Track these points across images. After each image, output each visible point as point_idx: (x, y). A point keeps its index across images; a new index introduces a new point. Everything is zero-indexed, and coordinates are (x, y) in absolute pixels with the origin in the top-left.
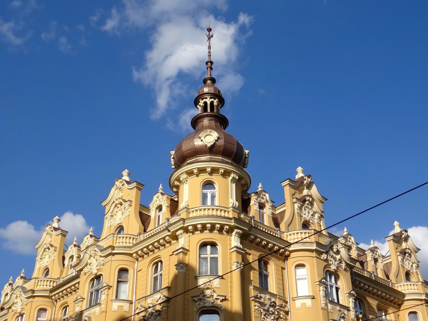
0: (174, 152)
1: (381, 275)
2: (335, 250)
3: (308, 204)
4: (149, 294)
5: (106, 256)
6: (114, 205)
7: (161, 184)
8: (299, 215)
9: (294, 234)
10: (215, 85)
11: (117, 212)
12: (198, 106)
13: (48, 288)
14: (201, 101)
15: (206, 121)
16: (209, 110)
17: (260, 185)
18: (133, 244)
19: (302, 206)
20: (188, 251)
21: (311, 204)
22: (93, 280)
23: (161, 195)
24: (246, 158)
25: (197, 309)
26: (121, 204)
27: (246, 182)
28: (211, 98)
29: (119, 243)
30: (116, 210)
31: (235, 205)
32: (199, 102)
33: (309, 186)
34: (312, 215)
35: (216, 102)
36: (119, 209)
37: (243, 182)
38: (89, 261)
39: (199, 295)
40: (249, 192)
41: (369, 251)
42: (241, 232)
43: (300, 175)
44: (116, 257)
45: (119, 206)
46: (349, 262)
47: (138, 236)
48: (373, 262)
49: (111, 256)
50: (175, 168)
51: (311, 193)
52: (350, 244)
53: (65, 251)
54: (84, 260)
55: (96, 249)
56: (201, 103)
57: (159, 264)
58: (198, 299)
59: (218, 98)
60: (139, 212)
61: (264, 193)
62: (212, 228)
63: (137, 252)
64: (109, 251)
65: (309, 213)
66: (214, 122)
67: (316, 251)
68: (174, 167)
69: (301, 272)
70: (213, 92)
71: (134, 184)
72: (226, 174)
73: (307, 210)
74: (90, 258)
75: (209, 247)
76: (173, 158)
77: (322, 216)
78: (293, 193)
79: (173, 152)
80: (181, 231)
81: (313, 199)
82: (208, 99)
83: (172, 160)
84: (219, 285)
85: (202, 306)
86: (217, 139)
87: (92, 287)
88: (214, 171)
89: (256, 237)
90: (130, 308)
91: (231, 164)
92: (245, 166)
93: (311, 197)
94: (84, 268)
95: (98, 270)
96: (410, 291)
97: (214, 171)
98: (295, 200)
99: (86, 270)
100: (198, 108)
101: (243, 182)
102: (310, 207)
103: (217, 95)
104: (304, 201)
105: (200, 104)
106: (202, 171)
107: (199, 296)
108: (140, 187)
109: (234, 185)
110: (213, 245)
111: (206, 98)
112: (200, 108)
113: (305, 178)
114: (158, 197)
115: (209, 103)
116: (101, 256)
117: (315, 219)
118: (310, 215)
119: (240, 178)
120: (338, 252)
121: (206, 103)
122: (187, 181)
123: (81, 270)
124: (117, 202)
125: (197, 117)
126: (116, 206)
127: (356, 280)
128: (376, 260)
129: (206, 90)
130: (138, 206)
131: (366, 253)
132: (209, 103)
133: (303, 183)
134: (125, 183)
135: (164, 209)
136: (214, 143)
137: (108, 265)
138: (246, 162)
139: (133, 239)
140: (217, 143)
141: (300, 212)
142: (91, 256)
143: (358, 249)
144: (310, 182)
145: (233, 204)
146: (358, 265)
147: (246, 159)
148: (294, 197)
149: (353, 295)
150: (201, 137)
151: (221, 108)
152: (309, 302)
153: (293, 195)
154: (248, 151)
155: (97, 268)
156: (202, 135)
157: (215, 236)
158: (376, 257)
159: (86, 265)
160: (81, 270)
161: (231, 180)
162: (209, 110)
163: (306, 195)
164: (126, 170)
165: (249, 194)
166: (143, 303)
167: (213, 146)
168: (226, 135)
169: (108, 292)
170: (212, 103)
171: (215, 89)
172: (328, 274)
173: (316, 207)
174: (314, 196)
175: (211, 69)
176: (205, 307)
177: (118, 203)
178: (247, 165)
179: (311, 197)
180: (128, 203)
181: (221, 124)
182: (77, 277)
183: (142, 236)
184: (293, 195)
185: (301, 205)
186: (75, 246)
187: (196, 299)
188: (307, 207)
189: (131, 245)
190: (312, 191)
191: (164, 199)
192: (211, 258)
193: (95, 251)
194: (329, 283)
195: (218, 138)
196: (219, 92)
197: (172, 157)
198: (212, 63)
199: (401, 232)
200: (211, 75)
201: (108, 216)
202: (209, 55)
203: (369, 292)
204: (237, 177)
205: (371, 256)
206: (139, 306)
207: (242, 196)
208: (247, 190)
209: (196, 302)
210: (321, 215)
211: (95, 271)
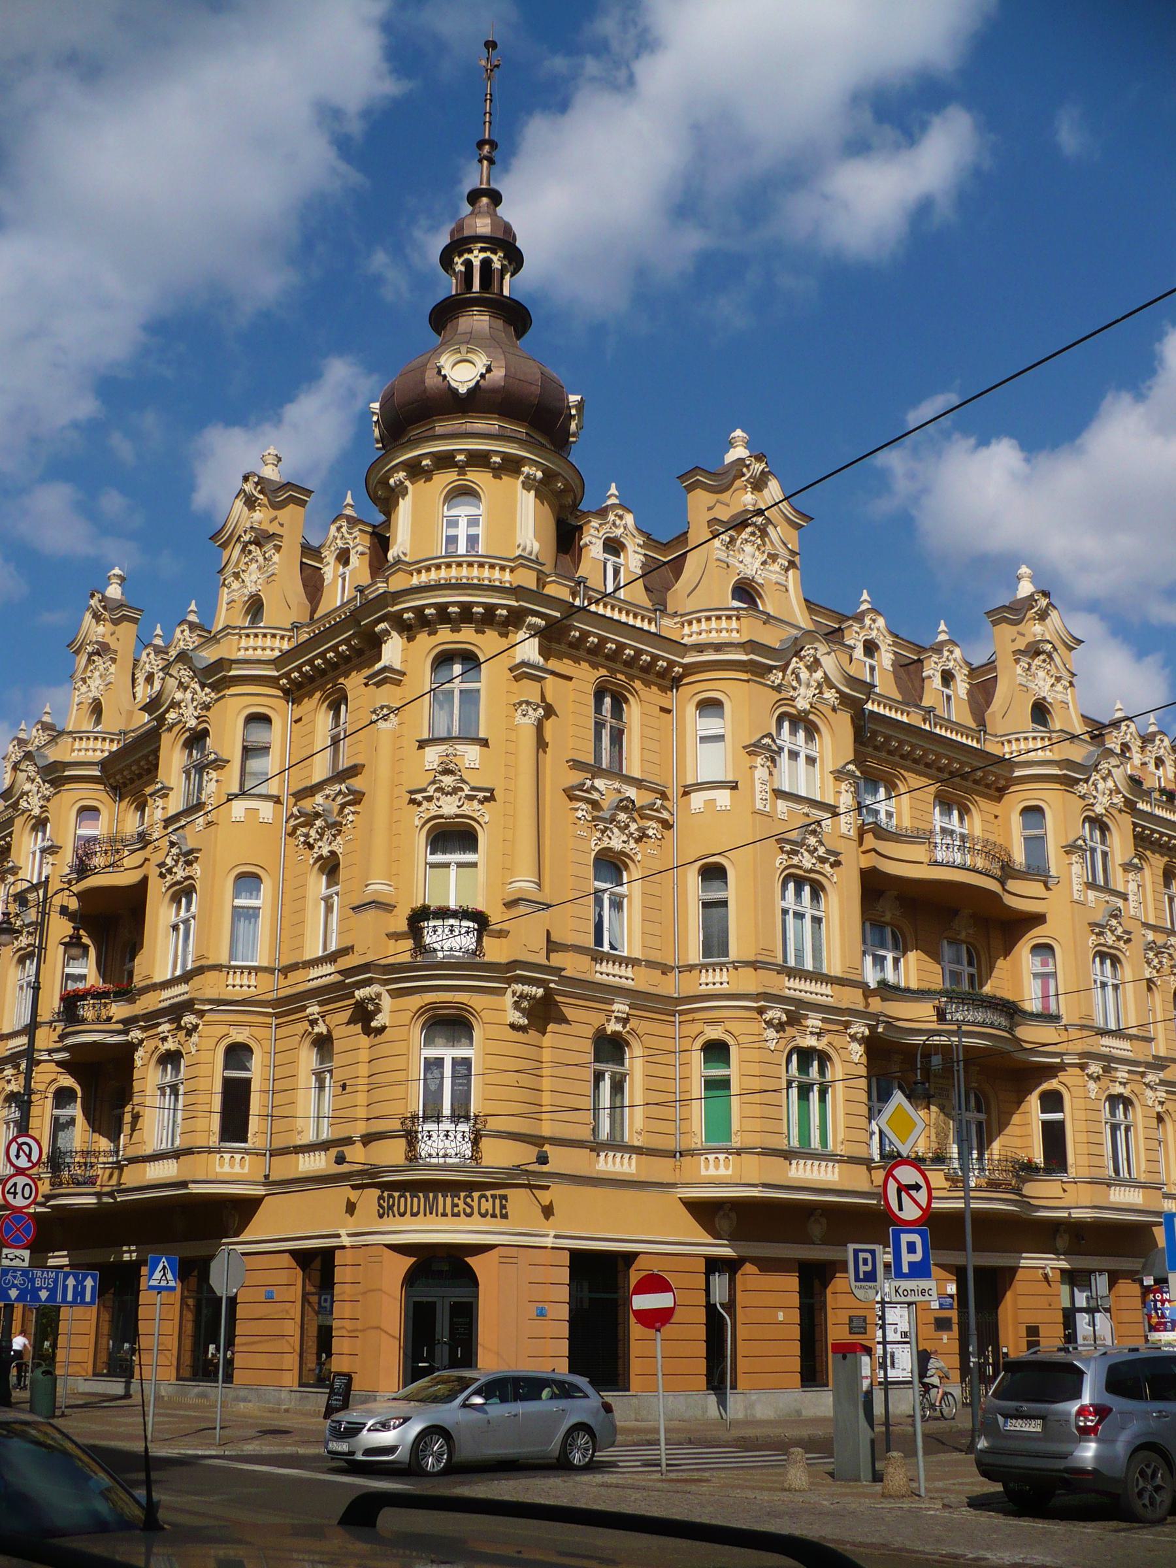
3: (753, 534)
6: (239, 547)
7: (349, 493)
10: (500, 210)
13: (99, 756)
16: (476, 286)
17: (613, 490)
20: (404, 674)
25: (423, 820)
28: (482, 250)
31: (528, 549)
33: (758, 485)
34: (764, 563)
39: (424, 786)
42: (541, 623)
43: (739, 452)
45: (252, 548)
46: (847, 690)
47: (292, 629)
50: (384, 447)
57: (343, 707)
58: (424, 798)
61: (620, 512)
62: (466, 615)
66: (487, 318)
72: (511, 466)
75: (457, 669)
80: (382, 626)
84: (477, 762)
85: (433, 813)
88: (479, 460)
89: (585, 634)
95: (197, 718)
106: (445, 461)
107: (424, 790)
109: (533, 492)
110: (470, 660)
111: (470, 251)
115: (476, 263)
119: (549, 475)
120: (815, 665)
126: (243, 550)
132: (476, 263)
135: (354, 559)
139: (282, 637)
145: (524, 550)
149: (851, 774)
154: (578, 398)
155: (196, 714)
157: (467, 635)
162: (476, 286)
170: (486, 263)
172: (786, 724)
176: (441, 817)
187: (419, 797)
189: (277, 653)
192: (461, 691)
198: (493, 144)
199: (1032, 595)
200: (488, 182)
204: (539, 474)
209: (420, 804)
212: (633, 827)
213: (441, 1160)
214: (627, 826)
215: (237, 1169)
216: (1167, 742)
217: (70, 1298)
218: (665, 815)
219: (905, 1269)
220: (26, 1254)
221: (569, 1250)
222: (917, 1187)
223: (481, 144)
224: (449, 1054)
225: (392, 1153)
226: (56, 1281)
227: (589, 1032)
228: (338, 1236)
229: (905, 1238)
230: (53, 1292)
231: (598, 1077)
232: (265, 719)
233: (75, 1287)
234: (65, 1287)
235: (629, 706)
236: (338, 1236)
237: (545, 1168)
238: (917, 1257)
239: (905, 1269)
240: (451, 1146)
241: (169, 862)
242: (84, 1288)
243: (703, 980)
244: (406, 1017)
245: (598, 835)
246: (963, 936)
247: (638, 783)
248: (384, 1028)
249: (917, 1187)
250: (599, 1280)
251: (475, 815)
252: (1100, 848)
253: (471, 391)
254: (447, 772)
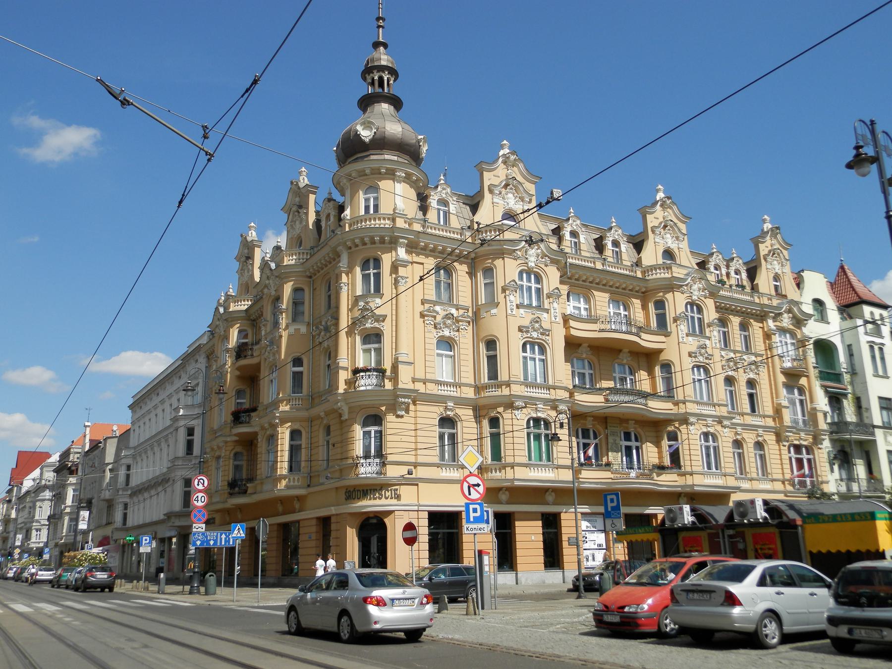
115: (376, 78)
132: (376, 78)
198: (384, 19)
215: (296, 483)
216: (741, 261)
219: (472, 519)
220: (204, 526)
222: (478, 485)
223: (378, 19)
229: (471, 507)
230: (215, 541)
231: (441, 437)
234: (221, 539)
238: (478, 514)
239: (472, 519)
246: (625, 361)
249: (478, 485)
252: (696, 316)
253: (371, 141)
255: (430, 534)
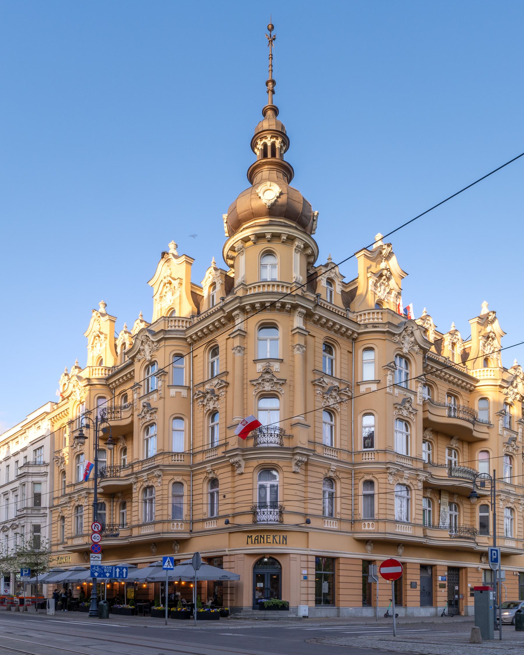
0: (227, 215)
1: (457, 360)
2: (409, 332)
4: (206, 380)
5: (159, 341)
6: (162, 284)
8: (373, 293)
9: (365, 314)
11: (166, 293)
12: (256, 150)
14: (259, 141)
15: (265, 172)
18: (186, 327)
19: (377, 282)
21: (389, 279)
22: (147, 366)
23: (213, 271)
24: (314, 220)
25: (256, 393)
26: (170, 283)
27: (313, 252)
29: (172, 327)
30: (165, 290)
32: (257, 143)
35: (278, 145)
36: (168, 288)
37: (309, 251)
38: (142, 348)
40: (316, 265)
41: (448, 334)
44: (168, 343)
45: (168, 285)
48: (451, 346)
49: (163, 341)
51: (389, 266)
52: (427, 326)
53: (116, 339)
54: (136, 346)
55: (147, 334)
56: (260, 146)
59: (281, 137)
60: (192, 292)
63: (191, 337)
64: (161, 336)
65: (385, 290)
67: (388, 332)
68: (227, 235)
69: (369, 356)
70: (274, 128)
71: (183, 258)
73: (383, 287)
74: (142, 344)
76: (226, 222)
77: (399, 294)
78: (369, 266)
79: (225, 216)
81: (391, 273)
82: (269, 138)
83: (225, 225)
85: (261, 390)
86: (278, 195)
87: (148, 374)
90: (189, 394)
91: (296, 228)
92: (313, 232)
93: (389, 271)
94: (137, 354)
95: (151, 356)
96: (486, 377)
97: (276, 236)
98: (369, 275)
99: (139, 356)
100: (256, 154)
101: (309, 251)
102: (387, 283)
103: (281, 133)
104: (381, 276)
105: (258, 146)
108: (190, 261)
112: (258, 153)
113: (384, 247)
114: (210, 273)
116: (153, 342)
117: (391, 297)
118: (386, 293)
121: (265, 145)
122: (243, 251)
123: (134, 356)
124: (166, 281)
125: (254, 165)
126: (165, 285)
127: (428, 365)
128: (454, 344)
129: (266, 125)
130: (190, 285)
131: (444, 336)
133: (381, 253)
134: (172, 257)
136: (276, 201)
137: (162, 350)
138: (314, 226)
139: (187, 322)
140: (279, 200)
141: (375, 289)
142: (142, 342)
143: (436, 332)
144: (390, 253)
146: (433, 349)
147: (315, 223)
148: (369, 270)
150: (259, 192)
151: (285, 152)
152: (374, 387)
153: (368, 268)
156: (260, 190)
158: (455, 341)
159: (139, 352)
160: (134, 356)
161: (295, 249)
163: (383, 269)
164: (173, 242)
165: (315, 268)
166: (201, 389)
167: (273, 205)
168: (290, 190)
169: (164, 378)
171: (277, 123)
173: (392, 283)
174: (393, 270)
175: (273, 92)
176: (265, 391)
177: (166, 282)
178: (314, 230)
179: (389, 271)
180: (178, 281)
181: (285, 175)
182: (131, 364)
183: (195, 318)
184: (368, 268)
185: (376, 280)
186: (126, 332)
187: (255, 383)
188: (383, 283)
189: (184, 328)
190: (390, 262)
191: (218, 275)
193: (146, 335)
194: (398, 367)
195: (281, 194)
196: (283, 127)
197: (225, 221)
201: (157, 297)
202: (270, 69)
203: (441, 378)
205: (449, 340)
206: (197, 392)
207: (308, 270)
208: (315, 260)
210: (398, 293)
211: (149, 358)
212: (338, 398)
213: (266, 522)
214: (336, 397)
217: (118, 576)
218: (350, 394)
221: (315, 556)
224: (268, 484)
225: (247, 520)
226: (112, 570)
227: (322, 476)
228: (225, 551)
232: (181, 356)
233: (119, 572)
234: (116, 572)
235: (335, 350)
236: (225, 551)
237: (308, 525)
240: (271, 517)
241: (143, 414)
242: (123, 572)
243: (364, 457)
244: (251, 469)
245: (325, 400)
247: (340, 380)
248: (242, 474)
250: (326, 567)
251: (279, 390)
254: (267, 372)
255: (316, 575)
